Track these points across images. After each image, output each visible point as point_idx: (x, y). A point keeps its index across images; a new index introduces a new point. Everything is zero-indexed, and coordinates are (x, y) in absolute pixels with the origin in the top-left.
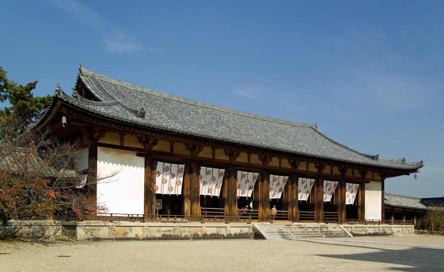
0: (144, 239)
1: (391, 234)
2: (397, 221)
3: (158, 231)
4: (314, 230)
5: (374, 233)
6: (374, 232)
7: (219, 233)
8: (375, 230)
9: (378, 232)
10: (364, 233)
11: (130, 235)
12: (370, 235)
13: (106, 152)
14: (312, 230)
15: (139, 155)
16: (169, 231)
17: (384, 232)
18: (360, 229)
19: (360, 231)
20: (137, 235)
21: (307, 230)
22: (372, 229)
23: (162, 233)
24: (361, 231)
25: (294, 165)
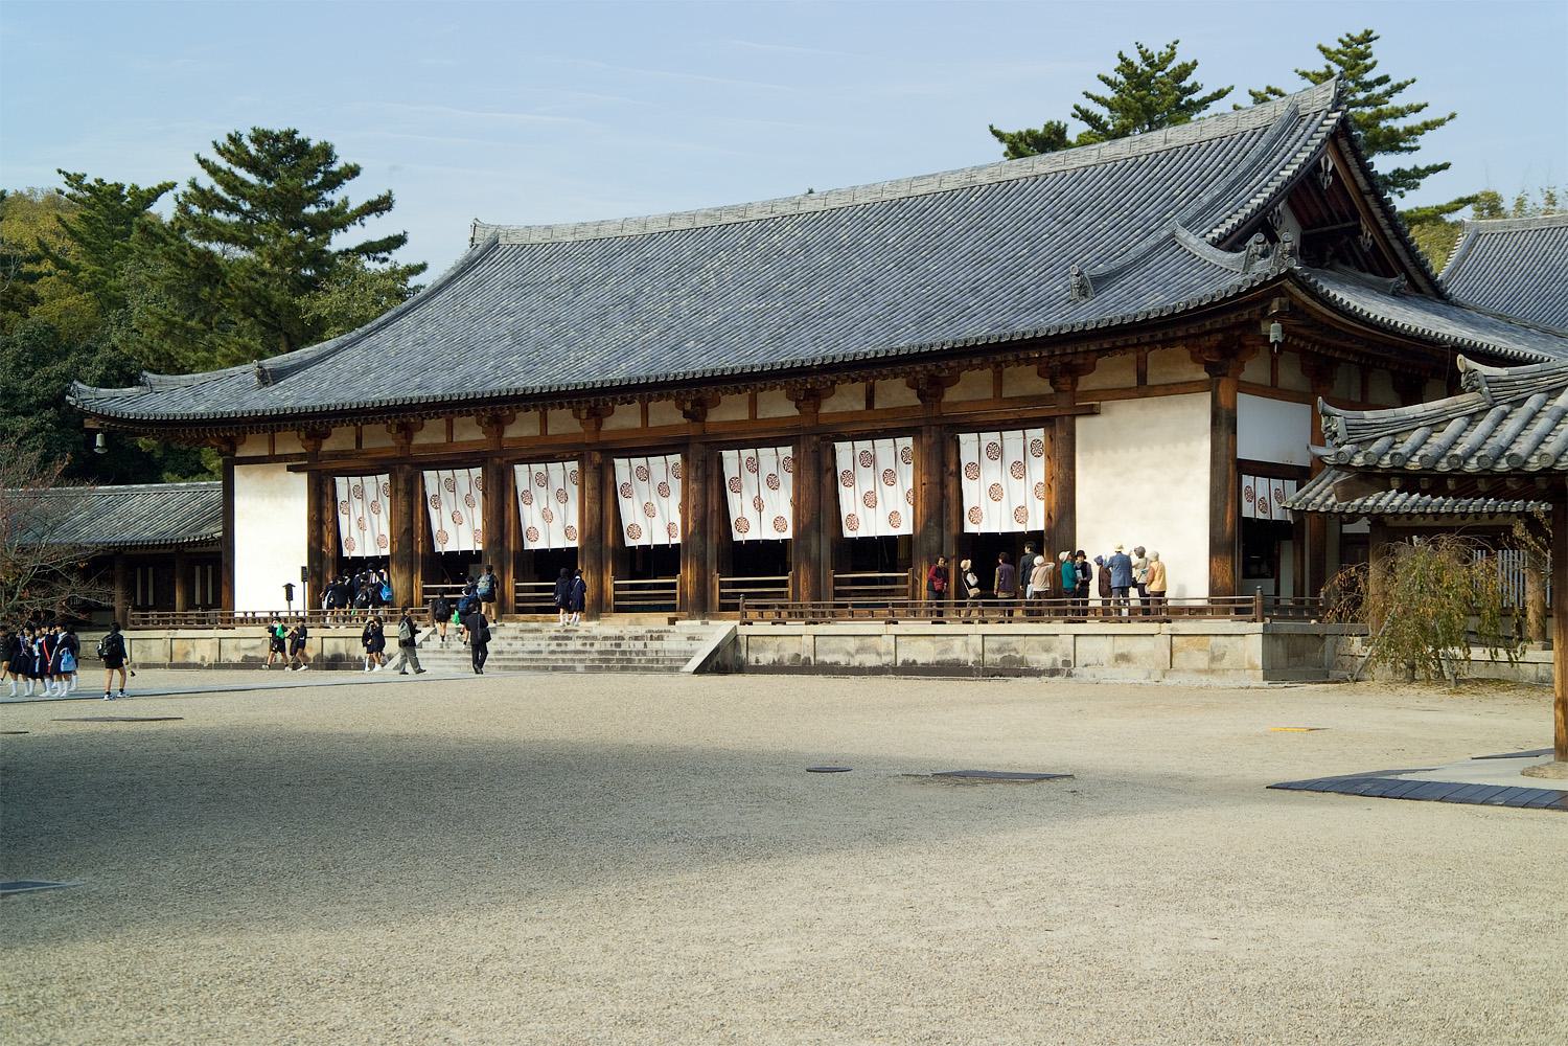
0: (210, 667)
1: (1053, 672)
2: (1065, 603)
3: (236, 648)
4: (592, 645)
5: (938, 663)
6: (938, 658)
7: (352, 653)
8: (946, 651)
9: (962, 657)
10: (871, 660)
11: (195, 658)
12: (909, 669)
13: (247, 476)
14: (585, 644)
15: (289, 469)
16: (253, 648)
17: (1009, 660)
18: (852, 644)
19: (848, 653)
20: (203, 659)
21: (566, 645)
22: (924, 643)
23: (242, 654)
24: (857, 652)
25: (696, 414)
